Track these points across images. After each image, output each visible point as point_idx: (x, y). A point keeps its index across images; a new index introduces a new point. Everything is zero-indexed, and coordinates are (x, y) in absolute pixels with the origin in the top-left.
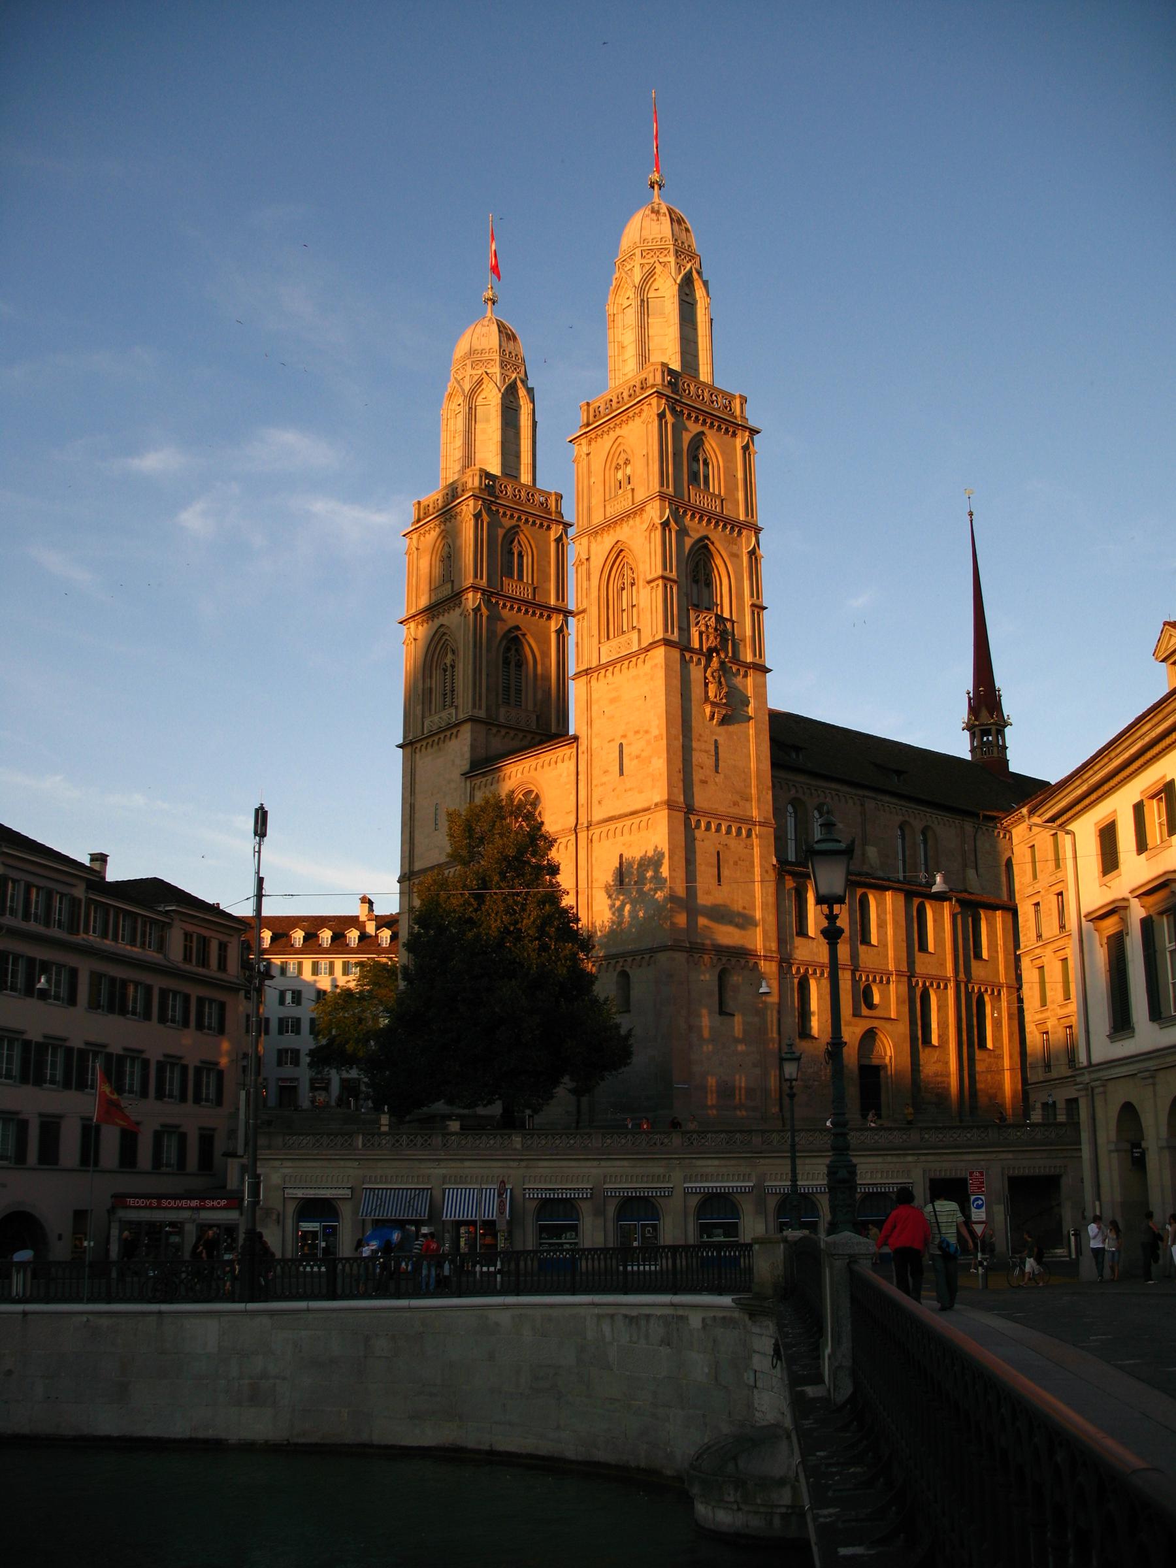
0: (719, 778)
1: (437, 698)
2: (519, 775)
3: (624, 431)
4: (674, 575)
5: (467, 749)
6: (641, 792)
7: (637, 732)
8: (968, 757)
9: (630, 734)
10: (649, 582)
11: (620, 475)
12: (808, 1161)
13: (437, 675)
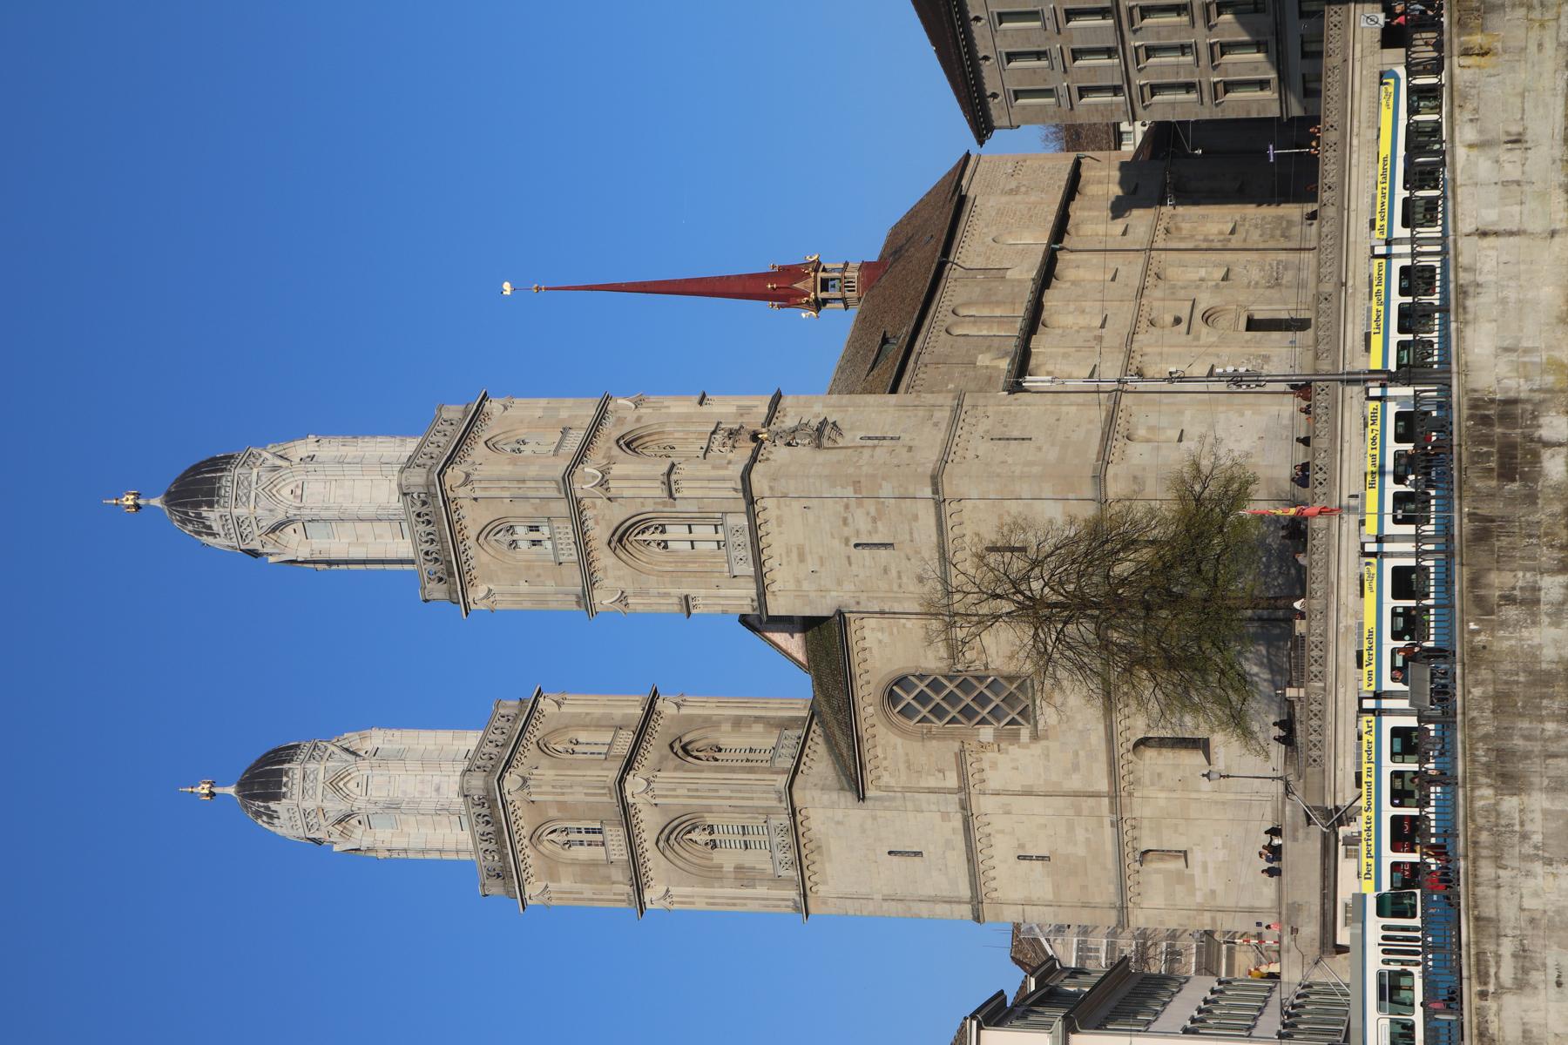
0: (906, 438)
1: (751, 858)
2: (870, 710)
3: (471, 532)
4: (665, 468)
5: (826, 798)
6: (916, 518)
7: (845, 521)
8: (854, 311)
9: (847, 531)
10: (671, 496)
11: (524, 545)
12: (1352, 239)
13: (718, 857)
